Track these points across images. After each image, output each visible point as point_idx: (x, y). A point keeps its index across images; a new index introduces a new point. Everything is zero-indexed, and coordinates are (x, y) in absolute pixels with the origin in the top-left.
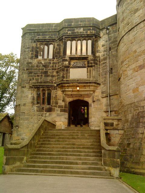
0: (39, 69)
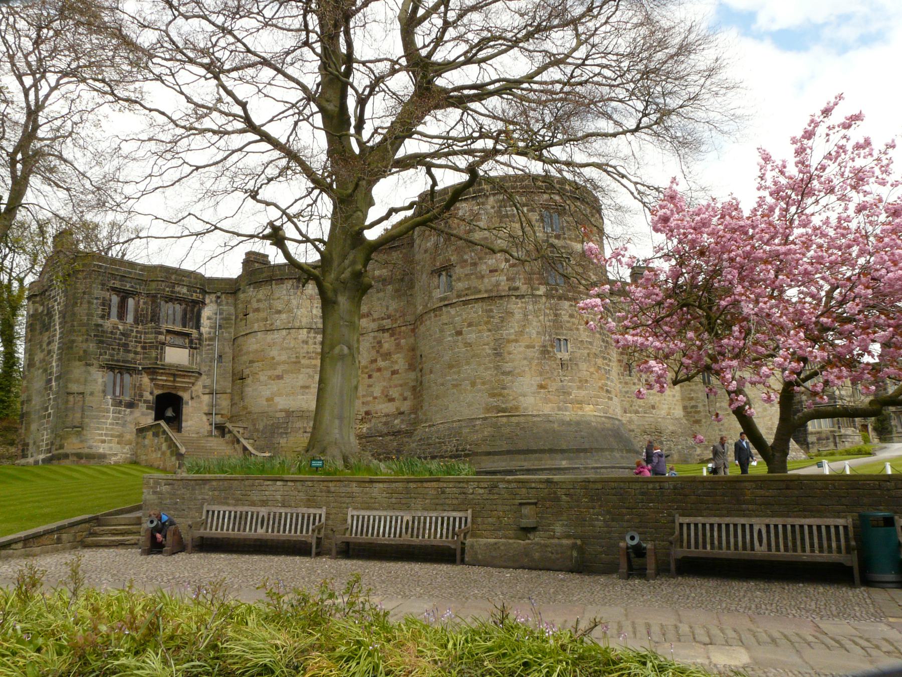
0: (115, 338)
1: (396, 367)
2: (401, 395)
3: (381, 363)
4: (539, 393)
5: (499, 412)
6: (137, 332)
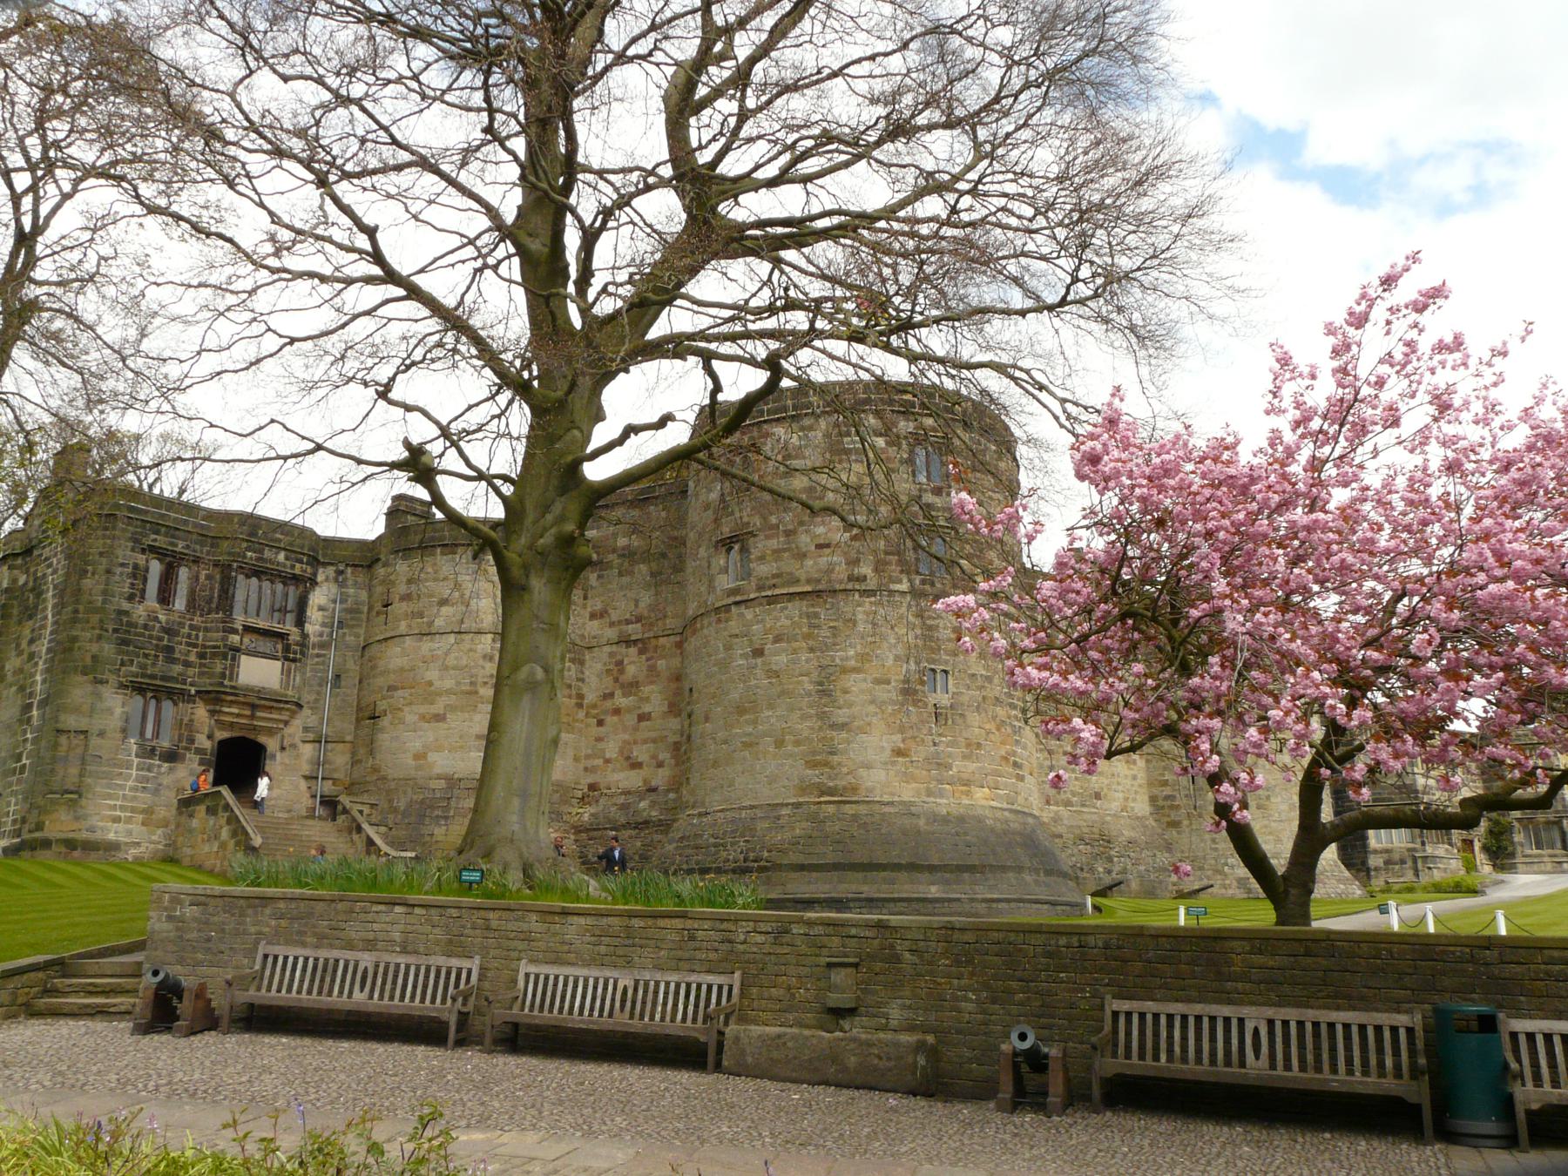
0: (151, 637)
1: (647, 708)
2: (654, 757)
3: (621, 701)
4: (894, 763)
5: (822, 794)
6: (192, 627)
